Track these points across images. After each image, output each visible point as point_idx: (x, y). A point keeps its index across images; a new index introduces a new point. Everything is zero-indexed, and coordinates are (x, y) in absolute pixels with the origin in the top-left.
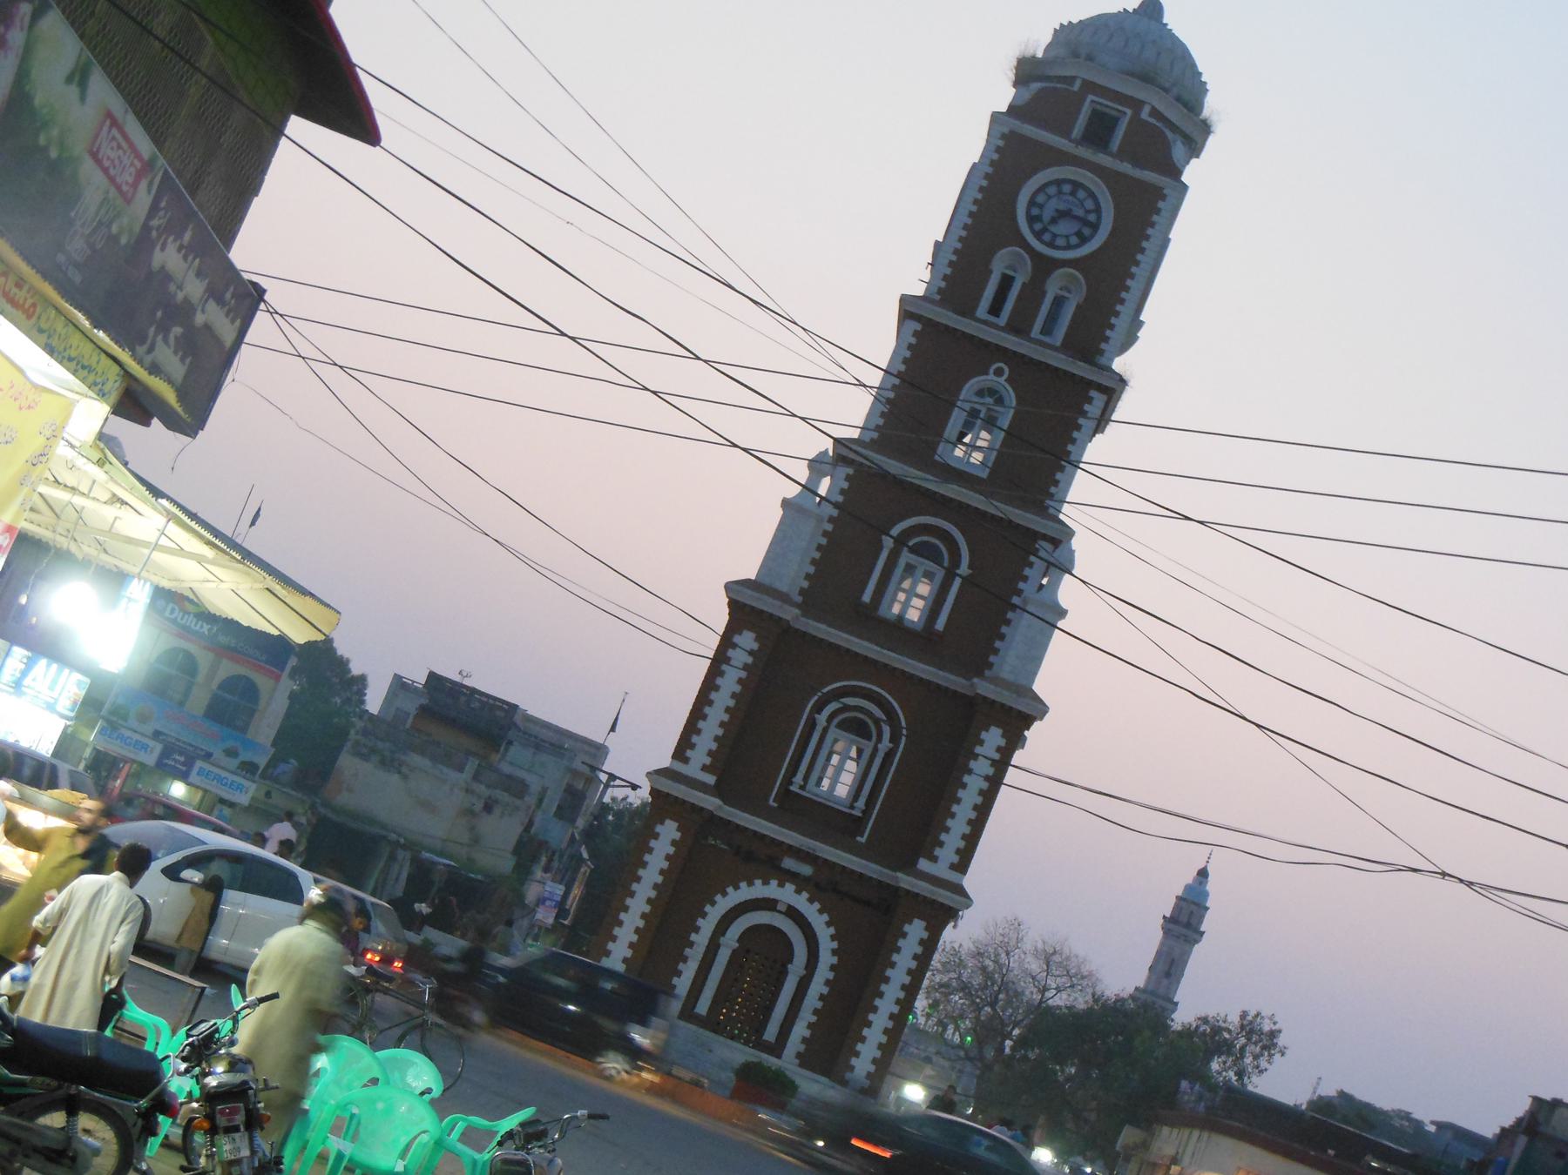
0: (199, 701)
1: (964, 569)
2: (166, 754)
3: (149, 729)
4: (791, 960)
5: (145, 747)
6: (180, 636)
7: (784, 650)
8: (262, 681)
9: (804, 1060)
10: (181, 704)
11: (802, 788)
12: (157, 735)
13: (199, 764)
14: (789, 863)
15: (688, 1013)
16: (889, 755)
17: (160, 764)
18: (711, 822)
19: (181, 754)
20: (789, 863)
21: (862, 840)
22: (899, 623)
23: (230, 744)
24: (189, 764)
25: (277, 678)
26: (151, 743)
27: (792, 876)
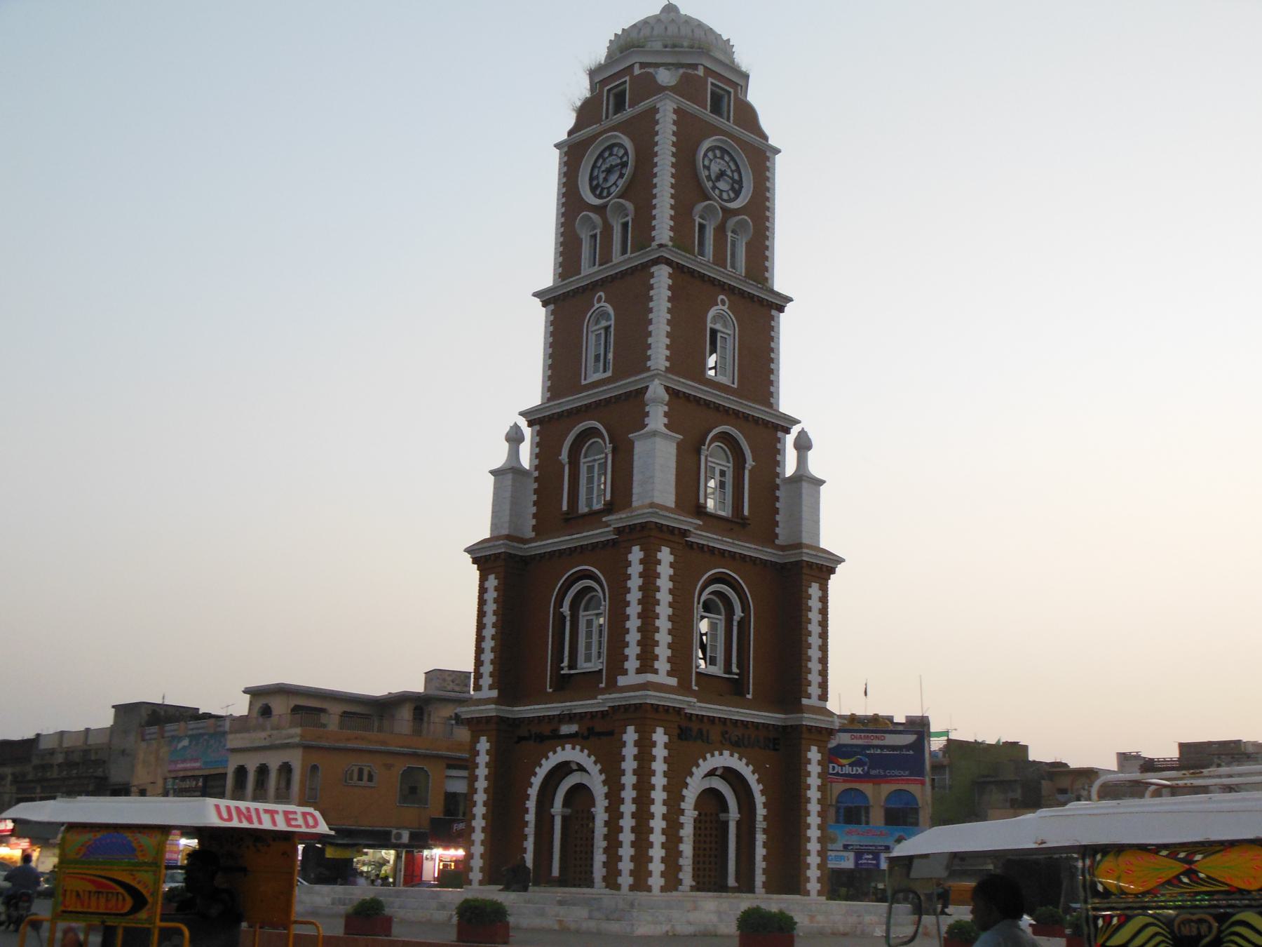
0: (877, 816)
1: (750, 462)
2: (859, 855)
3: (839, 845)
4: (593, 805)
5: (842, 858)
6: (845, 781)
7: (536, 573)
8: (914, 789)
9: (770, 888)
10: (867, 823)
11: (570, 667)
12: (846, 847)
13: (883, 856)
14: (566, 729)
15: (672, 882)
16: (743, 624)
17: (857, 864)
18: (501, 720)
19: (868, 853)
20: (566, 729)
21: (749, 696)
22: (584, 516)
23: (897, 835)
24: (876, 857)
25: (923, 783)
26: (845, 854)
27: (570, 738)
